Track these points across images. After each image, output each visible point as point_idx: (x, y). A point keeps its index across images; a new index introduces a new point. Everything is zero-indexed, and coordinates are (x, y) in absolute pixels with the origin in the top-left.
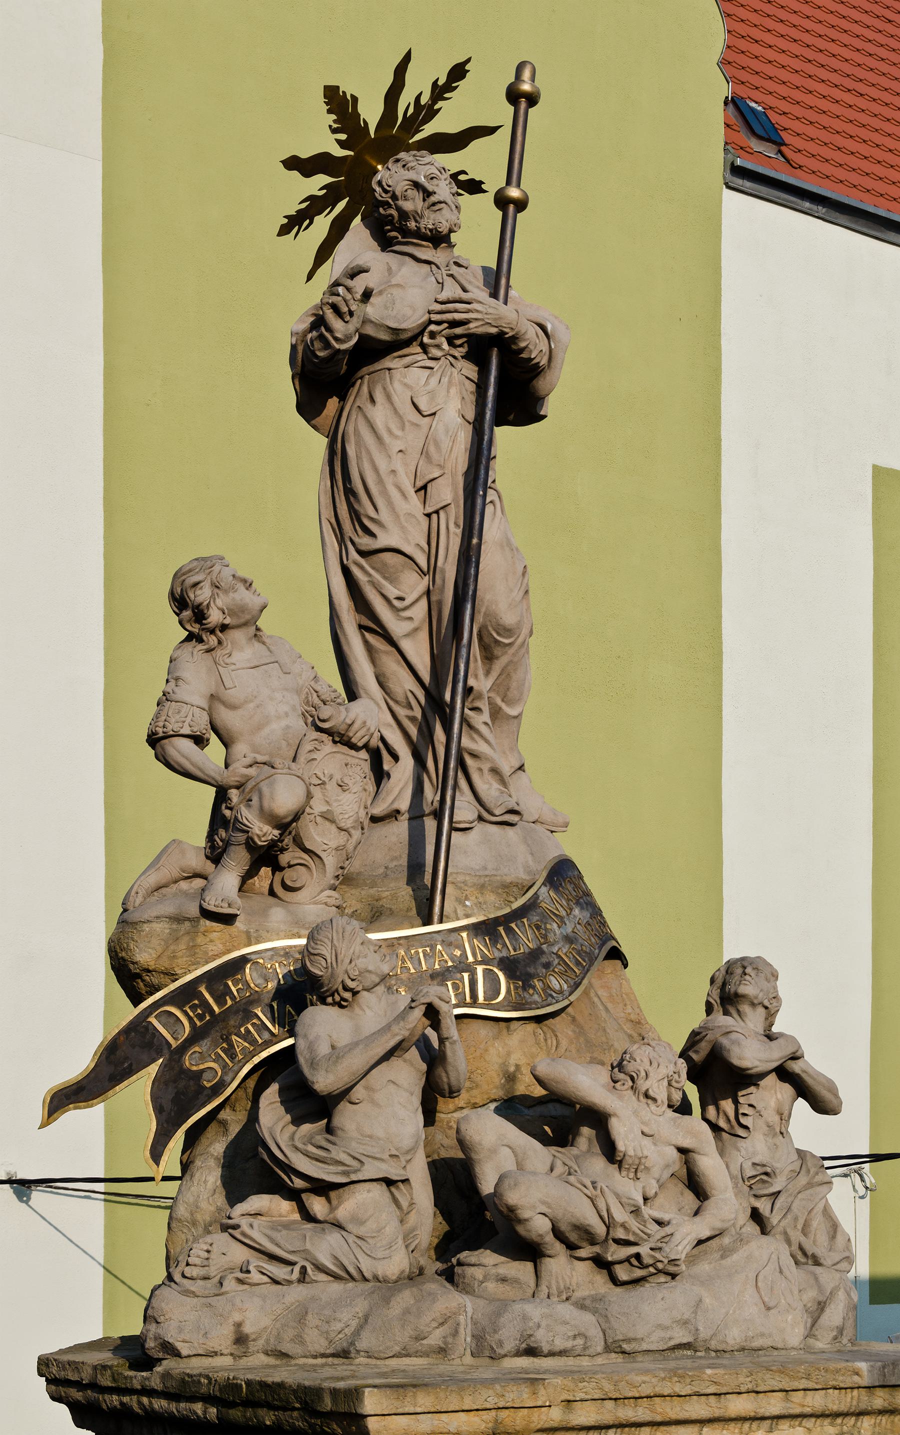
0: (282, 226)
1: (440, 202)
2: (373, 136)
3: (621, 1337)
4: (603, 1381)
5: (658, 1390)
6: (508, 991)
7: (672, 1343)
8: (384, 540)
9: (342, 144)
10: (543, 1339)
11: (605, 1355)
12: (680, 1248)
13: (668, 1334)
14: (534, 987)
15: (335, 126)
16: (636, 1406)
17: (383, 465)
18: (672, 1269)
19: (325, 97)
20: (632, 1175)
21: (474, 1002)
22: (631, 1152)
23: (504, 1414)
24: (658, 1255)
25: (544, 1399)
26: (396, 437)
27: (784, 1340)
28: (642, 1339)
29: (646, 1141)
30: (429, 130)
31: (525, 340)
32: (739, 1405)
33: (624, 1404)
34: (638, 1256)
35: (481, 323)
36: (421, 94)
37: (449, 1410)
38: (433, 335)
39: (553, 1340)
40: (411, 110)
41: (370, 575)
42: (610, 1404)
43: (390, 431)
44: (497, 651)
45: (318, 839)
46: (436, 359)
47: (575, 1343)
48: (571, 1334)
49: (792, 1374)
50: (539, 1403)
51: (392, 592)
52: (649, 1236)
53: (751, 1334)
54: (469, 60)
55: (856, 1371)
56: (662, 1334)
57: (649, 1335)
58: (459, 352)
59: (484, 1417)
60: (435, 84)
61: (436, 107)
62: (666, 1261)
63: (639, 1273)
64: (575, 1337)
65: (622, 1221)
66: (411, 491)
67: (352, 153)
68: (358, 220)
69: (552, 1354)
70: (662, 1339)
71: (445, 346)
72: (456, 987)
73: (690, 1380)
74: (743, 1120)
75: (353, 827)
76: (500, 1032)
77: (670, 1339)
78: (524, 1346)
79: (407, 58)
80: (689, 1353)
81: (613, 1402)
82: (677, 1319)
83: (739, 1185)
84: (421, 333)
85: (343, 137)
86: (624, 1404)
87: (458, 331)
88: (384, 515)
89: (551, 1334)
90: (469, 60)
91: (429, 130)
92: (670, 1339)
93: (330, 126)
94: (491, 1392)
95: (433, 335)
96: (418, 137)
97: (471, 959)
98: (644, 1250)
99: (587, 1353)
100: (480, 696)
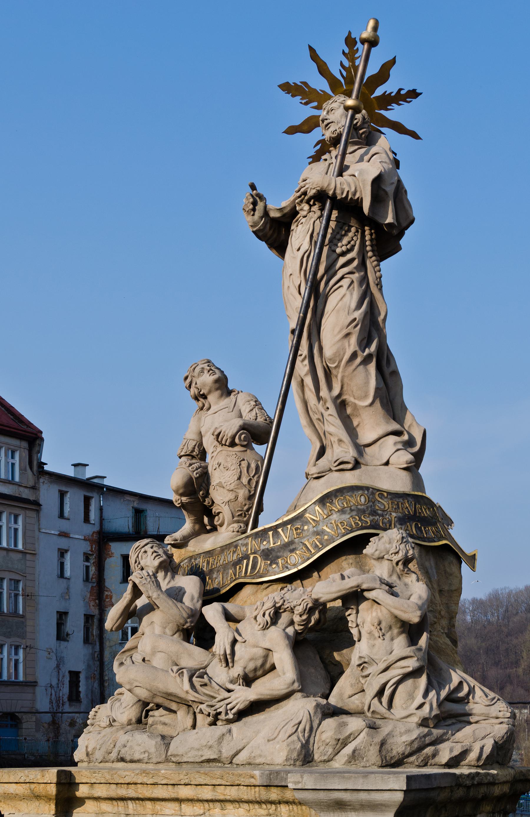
1: (332, 122)
4: (106, 773)
5: (134, 780)
7: (204, 758)
10: (126, 753)
11: (166, 764)
13: (200, 753)
16: (128, 788)
23: (33, 786)
25: (48, 779)
28: (182, 755)
32: (184, 792)
33: (121, 787)
36: (341, 62)
37: (4, 782)
39: (133, 754)
48: (142, 751)
49: (211, 775)
50: (45, 781)
53: (253, 755)
55: (253, 776)
56: (196, 753)
58: (315, 208)
59: (24, 787)
64: (145, 752)
65: (186, 690)
69: (132, 761)
70: (196, 756)
73: (152, 776)
80: (220, 765)
81: (115, 785)
82: (204, 745)
83: (354, 670)
84: (295, 207)
86: (121, 787)
89: (133, 750)
94: (22, 774)
99: (151, 761)
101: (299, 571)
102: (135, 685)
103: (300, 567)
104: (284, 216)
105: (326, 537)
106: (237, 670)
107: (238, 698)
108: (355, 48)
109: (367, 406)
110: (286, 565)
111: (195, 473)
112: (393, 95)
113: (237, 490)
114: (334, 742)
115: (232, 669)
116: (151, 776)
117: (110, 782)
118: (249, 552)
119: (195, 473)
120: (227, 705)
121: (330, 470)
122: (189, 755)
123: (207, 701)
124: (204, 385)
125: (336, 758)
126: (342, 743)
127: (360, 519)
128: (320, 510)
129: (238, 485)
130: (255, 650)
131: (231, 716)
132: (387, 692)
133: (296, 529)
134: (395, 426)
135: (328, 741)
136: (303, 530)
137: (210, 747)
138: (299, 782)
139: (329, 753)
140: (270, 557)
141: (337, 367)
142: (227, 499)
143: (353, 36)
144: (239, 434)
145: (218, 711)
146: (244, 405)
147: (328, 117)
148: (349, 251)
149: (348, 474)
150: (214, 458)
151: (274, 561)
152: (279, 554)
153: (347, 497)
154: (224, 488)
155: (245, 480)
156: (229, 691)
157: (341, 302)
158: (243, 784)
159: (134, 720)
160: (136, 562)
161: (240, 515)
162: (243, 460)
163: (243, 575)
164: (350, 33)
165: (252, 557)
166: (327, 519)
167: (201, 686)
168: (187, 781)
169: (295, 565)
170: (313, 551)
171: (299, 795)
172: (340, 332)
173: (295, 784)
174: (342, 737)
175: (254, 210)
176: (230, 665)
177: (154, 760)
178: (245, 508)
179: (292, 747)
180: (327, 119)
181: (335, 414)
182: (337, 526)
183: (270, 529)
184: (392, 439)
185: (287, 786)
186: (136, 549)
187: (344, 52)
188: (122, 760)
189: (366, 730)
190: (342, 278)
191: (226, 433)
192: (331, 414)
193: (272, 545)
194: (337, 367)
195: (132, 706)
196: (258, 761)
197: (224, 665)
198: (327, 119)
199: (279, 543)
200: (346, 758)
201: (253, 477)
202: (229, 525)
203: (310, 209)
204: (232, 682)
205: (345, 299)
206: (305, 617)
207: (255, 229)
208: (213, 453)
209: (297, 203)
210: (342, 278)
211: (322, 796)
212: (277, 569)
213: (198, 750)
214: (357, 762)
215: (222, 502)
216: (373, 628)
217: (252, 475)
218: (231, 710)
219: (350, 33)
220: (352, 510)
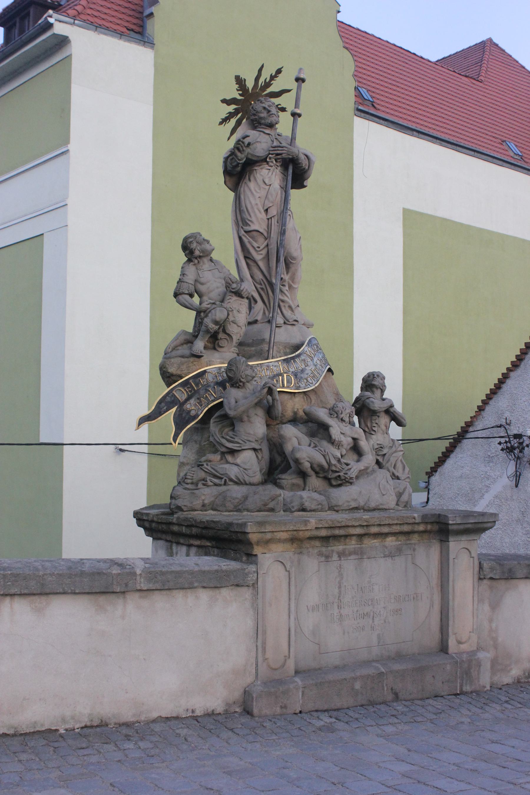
0: (220, 122)
2: (250, 92)
6: (295, 383)
7: (351, 507)
8: (253, 227)
9: (240, 95)
12: (354, 473)
15: (238, 89)
17: (253, 202)
18: (351, 481)
20: (337, 447)
21: (283, 386)
22: (337, 440)
24: (346, 476)
26: (258, 193)
29: (342, 436)
30: (269, 90)
34: (339, 476)
38: (270, 158)
40: (263, 84)
41: (248, 239)
43: (255, 191)
46: (271, 166)
47: (319, 507)
51: (256, 245)
52: (343, 469)
54: (283, 67)
56: (347, 504)
57: (343, 504)
60: (271, 75)
61: (271, 83)
62: (349, 478)
63: (339, 482)
66: (262, 211)
67: (243, 98)
68: (245, 120)
71: (274, 162)
74: (374, 429)
79: (263, 66)
84: (267, 157)
85: (241, 92)
87: (279, 157)
88: (253, 219)
90: (283, 67)
91: (269, 90)
92: (350, 506)
95: (270, 158)
96: (265, 93)
97: (282, 372)
98: (341, 474)
165: (285, 375)
168: (378, 523)
188: (304, 510)
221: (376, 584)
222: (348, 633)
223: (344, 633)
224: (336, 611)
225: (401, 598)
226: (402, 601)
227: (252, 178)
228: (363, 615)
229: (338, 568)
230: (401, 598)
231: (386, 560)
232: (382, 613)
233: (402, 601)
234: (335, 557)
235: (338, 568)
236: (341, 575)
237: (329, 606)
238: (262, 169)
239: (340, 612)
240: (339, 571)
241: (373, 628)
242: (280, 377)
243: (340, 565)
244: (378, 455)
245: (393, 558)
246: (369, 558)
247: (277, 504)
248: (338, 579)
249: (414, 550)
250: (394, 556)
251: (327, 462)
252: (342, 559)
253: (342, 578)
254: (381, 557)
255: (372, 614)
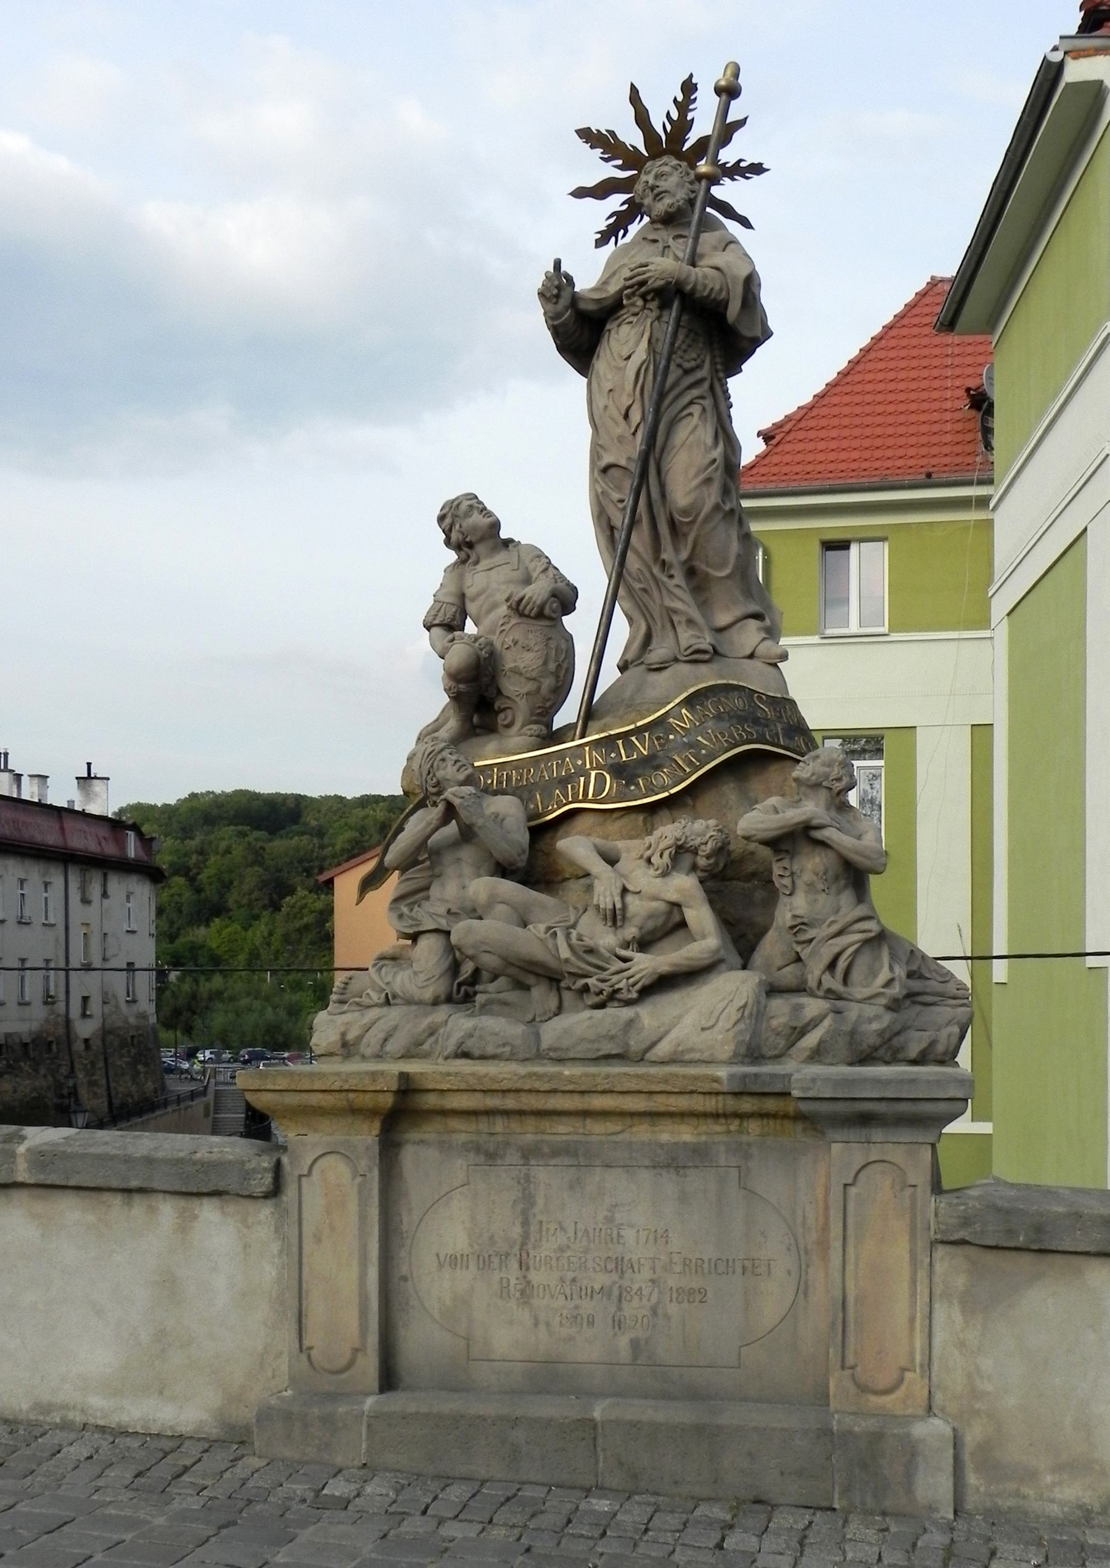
2: (647, 155)
3: (547, 1047)
7: (601, 1053)
13: (596, 1046)
14: (637, 785)
19: (581, 138)
25: (382, 1085)
27: (712, 1054)
31: (688, 284)
35: (653, 279)
40: (669, 128)
42: (479, 1095)
44: (685, 529)
45: (511, 688)
46: (635, 314)
50: (378, 1088)
58: (653, 305)
61: (689, 118)
66: (621, 419)
69: (483, 1058)
72: (573, 788)
75: (542, 677)
76: (605, 821)
77: (598, 1050)
78: (460, 1051)
85: (620, 162)
92: (598, 1050)
93: (601, 158)
97: (588, 766)
98: (589, 981)
100: (671, 566)
101: (671, 795)
102: (483, 948)
103: (673, 791)
104: (601, 310)
105: (704, 752)
106: (631, 931)
107: (643, 970)
108: (692, 97)
109: (723, 578)
110: (651, 787)
111: (483, 652)
112: (728, 165)
113: (542, 680)
114: (789, 1031)
115: (619, 931)
116: (546, 1079)
117: (475, 1088)
118: (588, 766)
119: (483, 652)
120: (628, 978)
121: (676, 660)
122: (579, 1048)
123: (596, 974)
124: (475, 528)
125: (791, 1051)
126: (799, 1033)
127: (744, 730)
128: (688, 715)
129: (542, 672)
130: (655, 904)
131: (634, 995)
132: (842, 964)
133: (658, 738)
134: (753, 608)
135: (780, 1029)
136: (668, 739)
137: (612, 1038)
138: (810, 1089)
139: (781, 1046)
140: (625, 774)
141: (693, 522)
142: (525, 690)
143: (694, 81)
144: (549, 602)
145: (617, 986)
146: (532, 561)
147: (658, 183)
148: (699, 367)
149: (703, 668)
150: (505, 633)
151: (631, 780)
152: (640, 771)
153: (722, 699)
154: (521, 674)
155: (552, 666)
156: (625, 960)
157: (692, 436)
158: (700, 1090)
159: (443, 997)
160: (429, 773)
161: (539, 714)
162: (550, 639)
163: (581, 797)
164: (691, 76)
165: (593, 774)
166: (701, 727)
167: (585, 952)
168: (607, 1087)
169: (664, 788)
170: (688, 770)
171: (804, 1107)
172: (697, 475)
173: (804, 1092)
174: (799, 1024)
175: (557, 296)
176: (619, 923)
177: (521, 1056)
178: (548, 704)
179: (741, 1038)
180: (658, 187)
181: (683, 584)
182: (716, 737)
183: (619, 736)
184: (753, 624)
185: (790, 1094)
186: (429, 754)
187: (675, 100)
188: (466, 1055)
189: (831, 1015)
190: (691, 403)
191: (534, 599)
192: (678, 583)
193: (624, 759)
194: (693, 522)
195: (440, 977)
196: (687, 1057)
197: (609, 924)
198: (658, 187)
199: (635, 757)
200: (808, 1053)
201: (563, 661)
202: (523, 726)
203: (645, 305)
204: (626, 945)
205: (697, 433)
206: (712, 861)
207: (556, 323)
208: (502, 625)
209: (626, 295)
210: (691, 403)
211: (840, 1107)
212: (637, 792)
213: (593, 1041)
214: (822, 1058)
215: (517, 693)
216: (815, 878)
217: (561, 660)
218: (633, 985)
219: (691, 76)
220: (731, 718)
221: (631, 1226)
222: (548, 1324)
223: (536, 1324)
224: (513, 1273)
225: (706, 1266)
226: (706, 1271)
227: (601, 355)
228: (589, 1290)
229: (522, 1181)
230: (706, 1266)
231: (661, 1175)
232: (645, 1292)
233: (706, 1271)
234: (513, 1157)
235: (522, 1181)
236: (528, 1199)
237: (496, 1260)
238: (619, 326)
239: (525, 1277)
240: (524, 1189)
241: (618, 1324)
242: (582, 779)
243: (527, 1177)
244: (798, 943)
245: (682, 1172)
246: (608, 1166)
247: (437, 1041)
248: (520, 1206)
249: (747, 1157)
250: (684, 1167)
251: (553, 956)
252: (532, 1162)
253: (533, 1204)
254: (646, 1167)
255: (616, 1292)
